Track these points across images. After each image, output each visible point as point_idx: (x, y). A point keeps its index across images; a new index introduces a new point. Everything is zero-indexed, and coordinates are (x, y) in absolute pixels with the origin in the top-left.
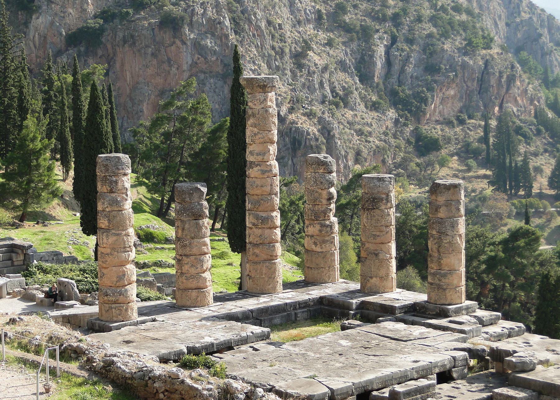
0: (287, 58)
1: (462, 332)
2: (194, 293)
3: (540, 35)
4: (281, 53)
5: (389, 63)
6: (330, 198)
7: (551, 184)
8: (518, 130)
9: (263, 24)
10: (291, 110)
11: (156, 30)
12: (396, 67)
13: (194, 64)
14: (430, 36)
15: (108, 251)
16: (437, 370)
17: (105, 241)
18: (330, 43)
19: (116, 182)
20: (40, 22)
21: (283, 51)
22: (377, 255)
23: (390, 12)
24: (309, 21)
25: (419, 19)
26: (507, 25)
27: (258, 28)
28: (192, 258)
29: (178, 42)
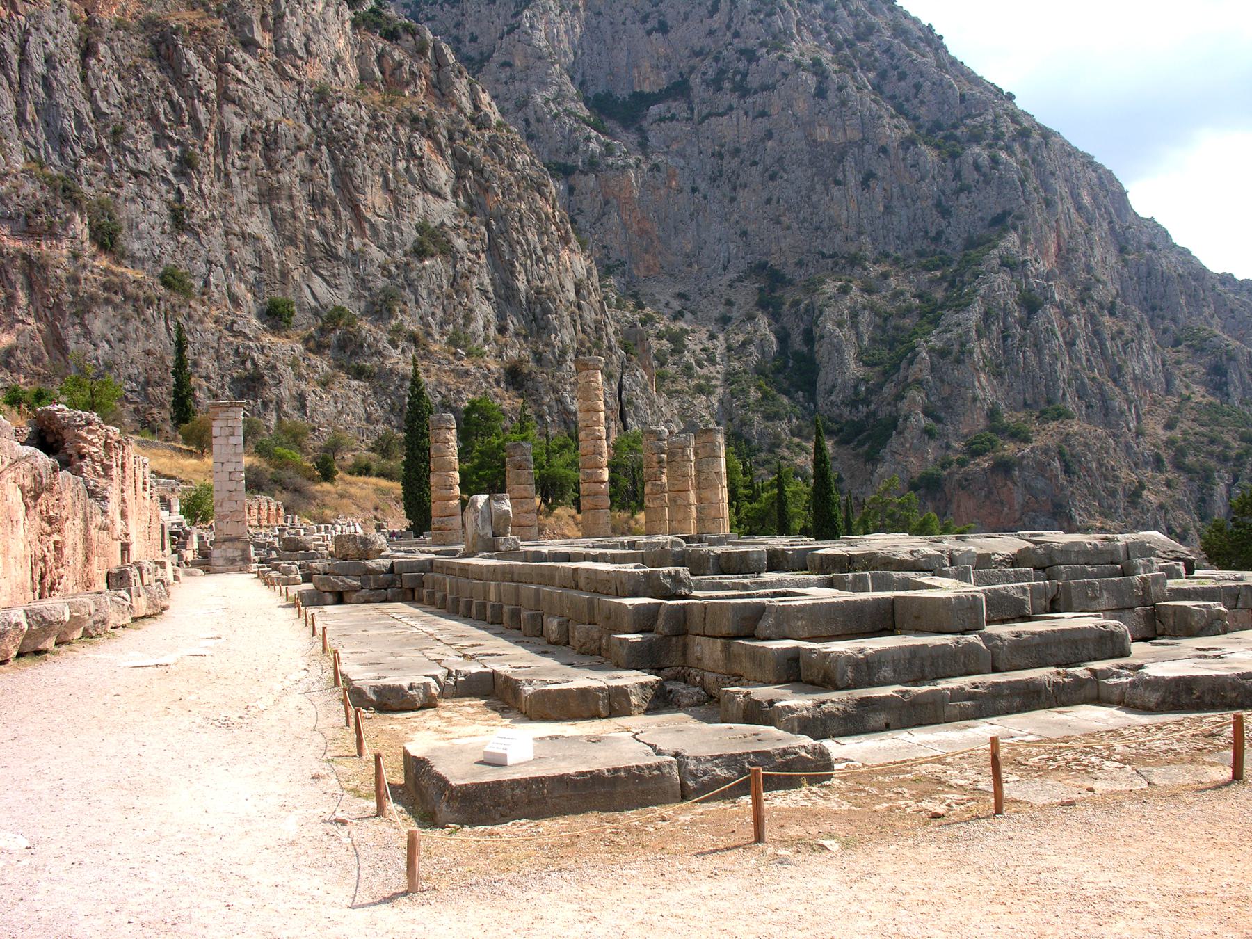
0: (1120, 496)
4: (1113, 494)
6: (660, 461)
9: (1094, 465)
13: (1026, 505)
18: (1168, 484)
23: (1232, 454)
24: (1147, 463)
27: (1089, 469)
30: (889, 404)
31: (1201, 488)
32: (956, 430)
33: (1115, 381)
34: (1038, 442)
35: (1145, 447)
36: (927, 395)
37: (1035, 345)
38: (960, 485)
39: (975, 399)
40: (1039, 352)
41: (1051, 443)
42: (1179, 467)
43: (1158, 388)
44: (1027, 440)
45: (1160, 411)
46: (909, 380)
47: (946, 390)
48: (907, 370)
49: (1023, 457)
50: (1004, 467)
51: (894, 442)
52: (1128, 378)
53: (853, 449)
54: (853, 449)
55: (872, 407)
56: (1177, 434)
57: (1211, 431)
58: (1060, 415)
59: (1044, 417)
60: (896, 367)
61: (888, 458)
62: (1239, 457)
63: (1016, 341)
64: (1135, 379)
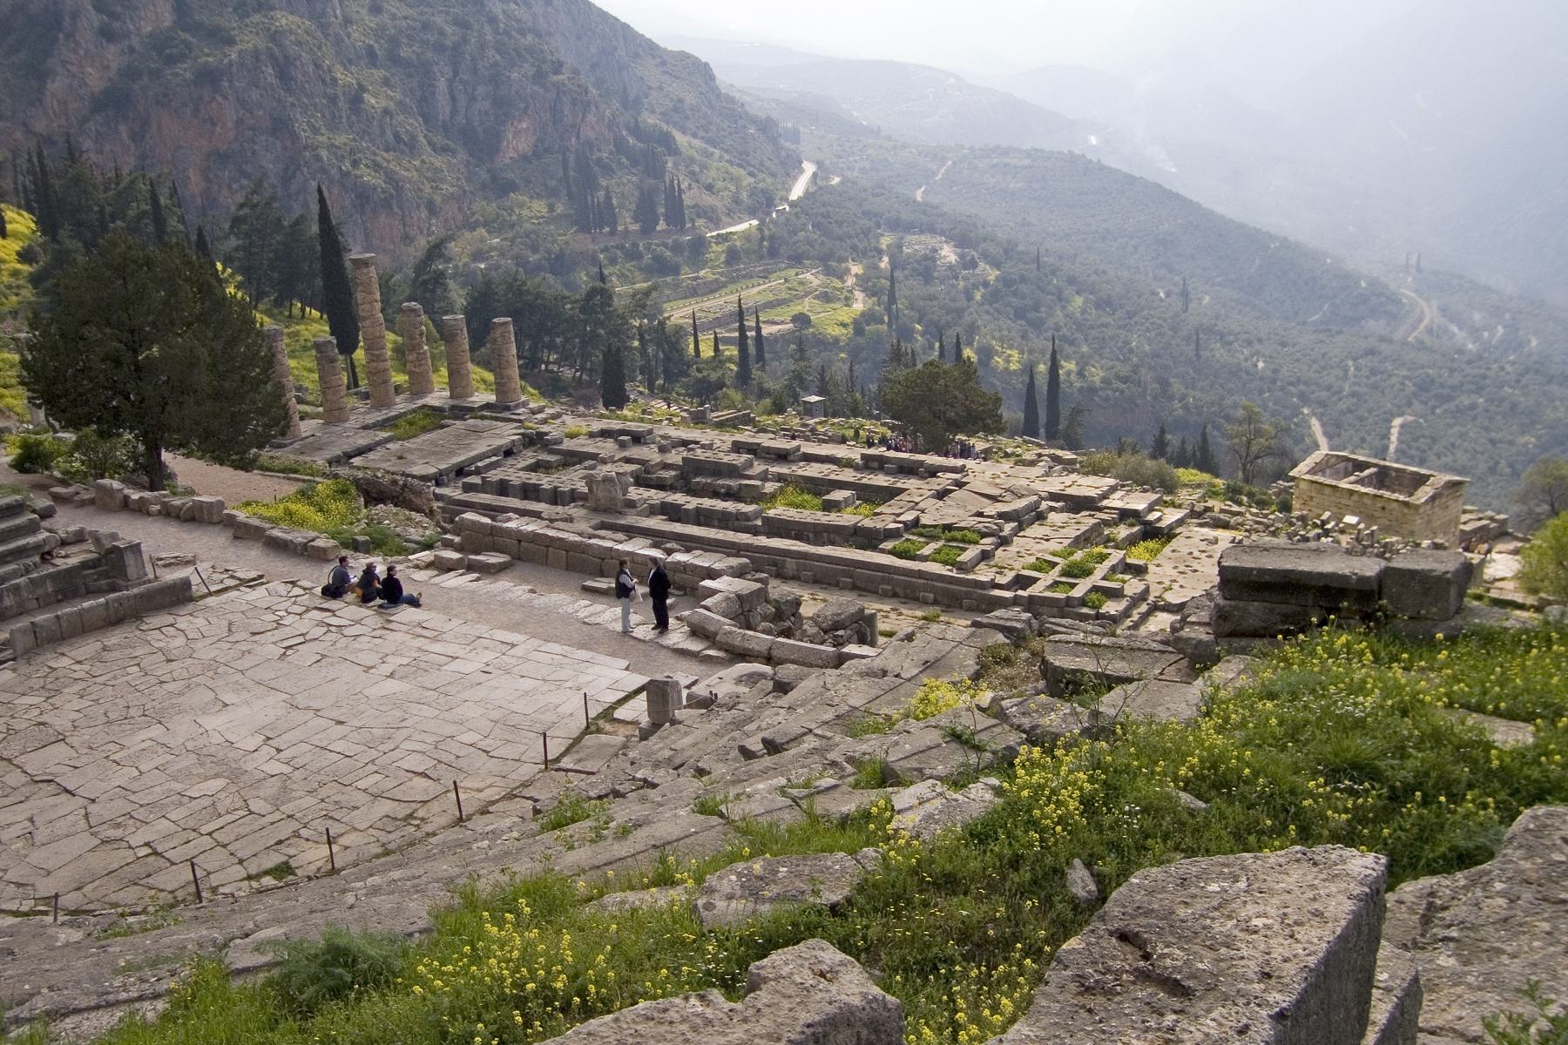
1: (520, 421)
4: (333, 100)
5: (453, 99)
7: (636, 219)
8: (598, 161)
9: (311, 69)
10: (355, 164)
12: (462, 103)
13: (240, 121)
14: (496, 64)
18: (386, 82)
20: (56, 85)
25: (482, 46)
26: (579, 38)
27: (305, 74)
29: (219, 98)
34: (249, 41)
38: (158, 102)
41: (261, 43)
42: (394, 60)
44: (231, 42)
49: (231, 64)
50: (210, 77)
61: (59, 69)
62: (456, 47)
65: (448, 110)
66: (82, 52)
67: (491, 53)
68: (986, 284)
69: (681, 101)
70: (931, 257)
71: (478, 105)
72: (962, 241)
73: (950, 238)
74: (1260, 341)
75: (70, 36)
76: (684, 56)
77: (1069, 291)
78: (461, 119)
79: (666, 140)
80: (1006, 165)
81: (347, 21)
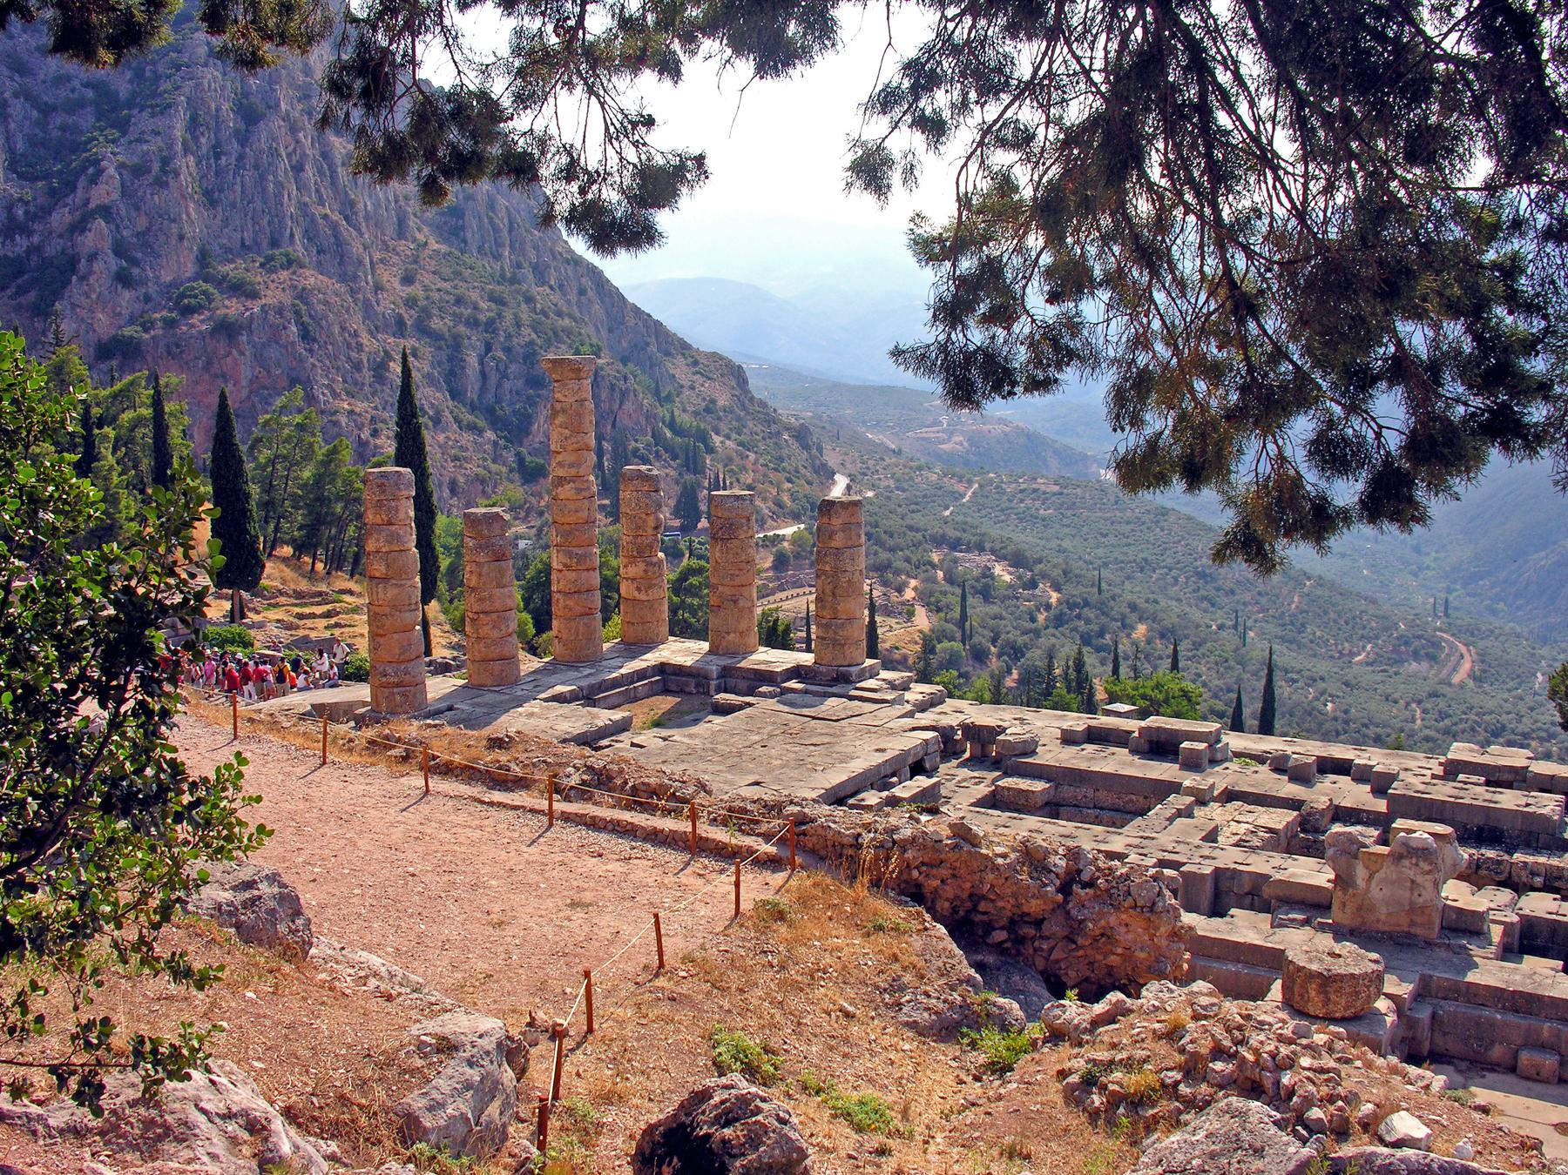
2: (497, 666)
3: (648, 344)
4: (357, 367)
7: (676, 513)
9: (337, 330)
10: (375, 433)
11: (208, 340)
12: (493, 378)
14: (532, 343)
15: (387, 610)
16: (910, 761)
17: (381, 595)
19: (397, 511)
21: (361, 361)
22: (735, 602)
25: (518, 325)
26: (610, 331)
27: (331, 335)
28: (494, 616)
30: (61, 236)
31: (450, 359)
32: (158, 278)
33: (346, 218)
35: (386, 306)
36: (118, 227)
37: (256, 167)
39: (181, 238)
40: (262, 178)
41: (287, 299)
42: (423, 330)
43: (390, 230)
44: (254, 295)
45: (395, 259)
46: (92, 205)
47: (142, 222)
48: (87, 189)
50: (227, 330)
51: (75, 289)
52: (361, 215)
53: (10, 297)
54: (10, 297)
55: (36, 239)
56: (415, 290)
57: (455, 287)
58: (290, 263)
59: (269, 265)
60: (72, 187)
62: (491, 322)
63: (233, 160)
64: (367, 217)
65: (477, 387)
66: (94, 296)
67: (526, 331)
68: (1048, 607)
69: (713, 401)
70: (987, 573)
71: (507, 385)
72: (1017, 560)
73: (1000, 558)
74: (1322, 679)
75: (83, 279)
76: (715, 357)
77: (1133, 617)
78: (490, 398)
79: (703, 437)
80: (1035, 491)
81: (378, 288)
